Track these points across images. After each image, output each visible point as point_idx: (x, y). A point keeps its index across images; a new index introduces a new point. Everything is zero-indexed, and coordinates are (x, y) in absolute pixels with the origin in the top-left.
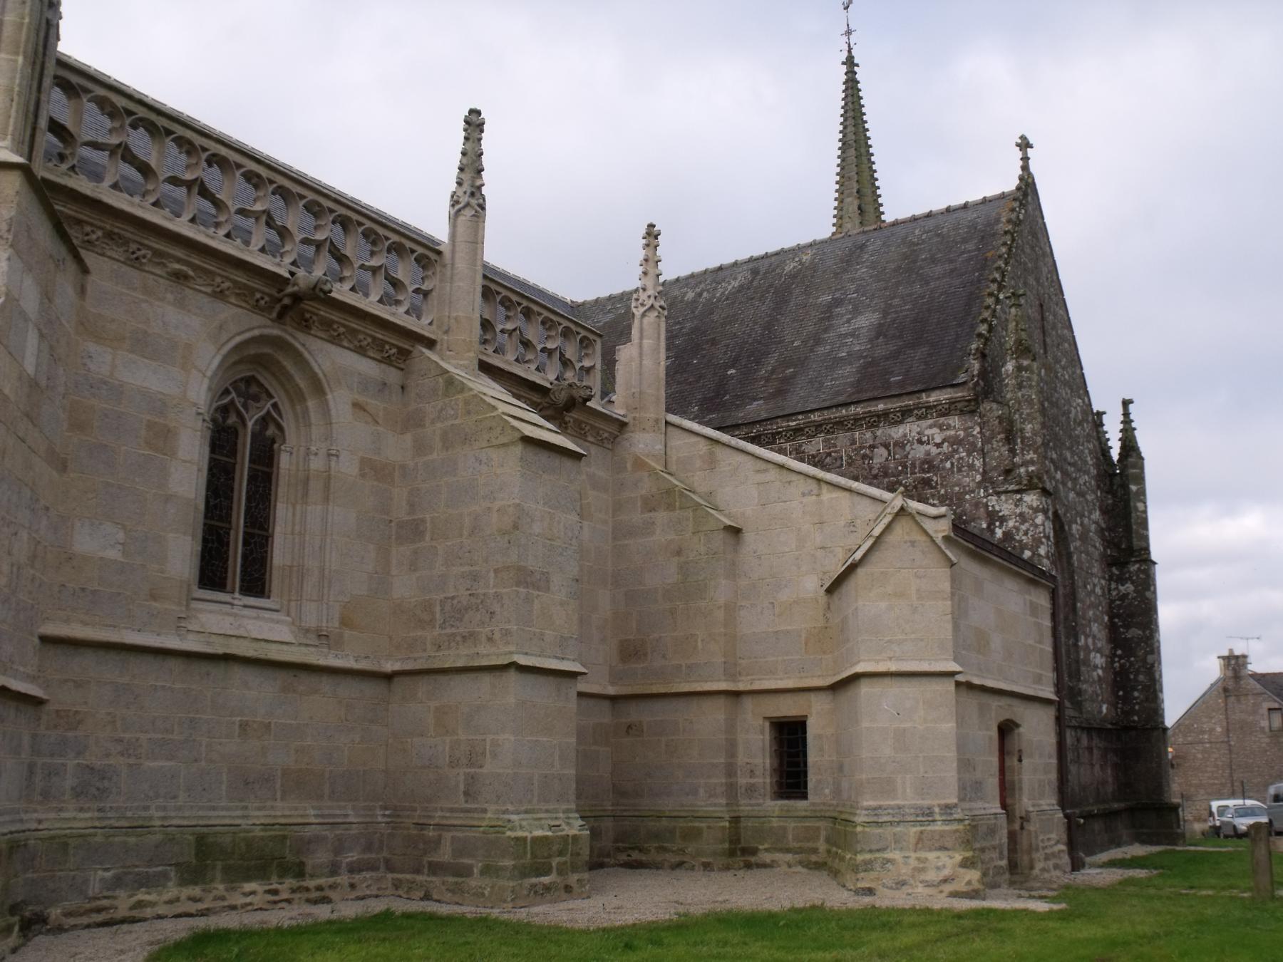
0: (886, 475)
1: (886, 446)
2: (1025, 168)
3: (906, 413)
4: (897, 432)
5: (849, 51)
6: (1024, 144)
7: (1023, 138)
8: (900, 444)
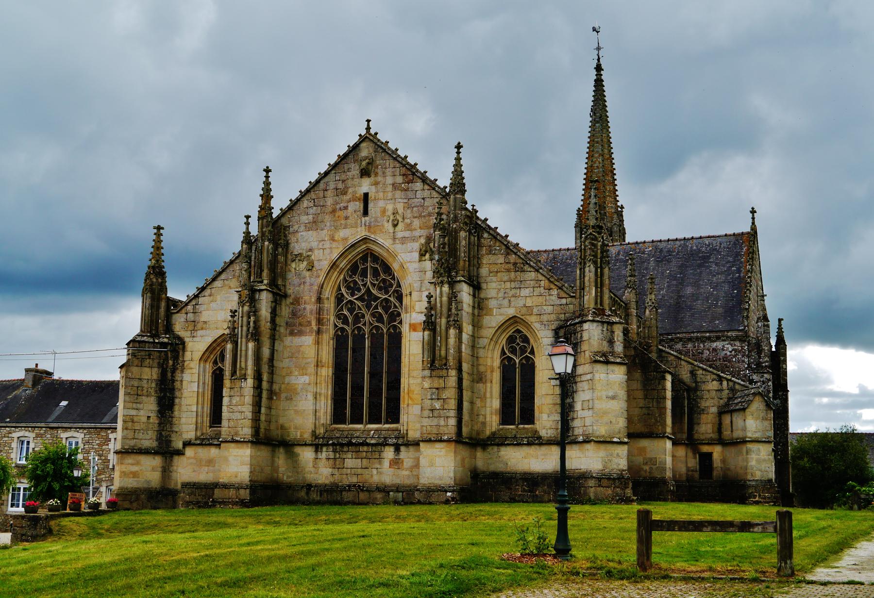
0: (708, 361)
1: (709, 350)
2: (753, 223)
3: (718, 338)
4: (714, 345)
5: (599, 60)
6: (753, 212)
7: (753, 208)
8: (715, 350)
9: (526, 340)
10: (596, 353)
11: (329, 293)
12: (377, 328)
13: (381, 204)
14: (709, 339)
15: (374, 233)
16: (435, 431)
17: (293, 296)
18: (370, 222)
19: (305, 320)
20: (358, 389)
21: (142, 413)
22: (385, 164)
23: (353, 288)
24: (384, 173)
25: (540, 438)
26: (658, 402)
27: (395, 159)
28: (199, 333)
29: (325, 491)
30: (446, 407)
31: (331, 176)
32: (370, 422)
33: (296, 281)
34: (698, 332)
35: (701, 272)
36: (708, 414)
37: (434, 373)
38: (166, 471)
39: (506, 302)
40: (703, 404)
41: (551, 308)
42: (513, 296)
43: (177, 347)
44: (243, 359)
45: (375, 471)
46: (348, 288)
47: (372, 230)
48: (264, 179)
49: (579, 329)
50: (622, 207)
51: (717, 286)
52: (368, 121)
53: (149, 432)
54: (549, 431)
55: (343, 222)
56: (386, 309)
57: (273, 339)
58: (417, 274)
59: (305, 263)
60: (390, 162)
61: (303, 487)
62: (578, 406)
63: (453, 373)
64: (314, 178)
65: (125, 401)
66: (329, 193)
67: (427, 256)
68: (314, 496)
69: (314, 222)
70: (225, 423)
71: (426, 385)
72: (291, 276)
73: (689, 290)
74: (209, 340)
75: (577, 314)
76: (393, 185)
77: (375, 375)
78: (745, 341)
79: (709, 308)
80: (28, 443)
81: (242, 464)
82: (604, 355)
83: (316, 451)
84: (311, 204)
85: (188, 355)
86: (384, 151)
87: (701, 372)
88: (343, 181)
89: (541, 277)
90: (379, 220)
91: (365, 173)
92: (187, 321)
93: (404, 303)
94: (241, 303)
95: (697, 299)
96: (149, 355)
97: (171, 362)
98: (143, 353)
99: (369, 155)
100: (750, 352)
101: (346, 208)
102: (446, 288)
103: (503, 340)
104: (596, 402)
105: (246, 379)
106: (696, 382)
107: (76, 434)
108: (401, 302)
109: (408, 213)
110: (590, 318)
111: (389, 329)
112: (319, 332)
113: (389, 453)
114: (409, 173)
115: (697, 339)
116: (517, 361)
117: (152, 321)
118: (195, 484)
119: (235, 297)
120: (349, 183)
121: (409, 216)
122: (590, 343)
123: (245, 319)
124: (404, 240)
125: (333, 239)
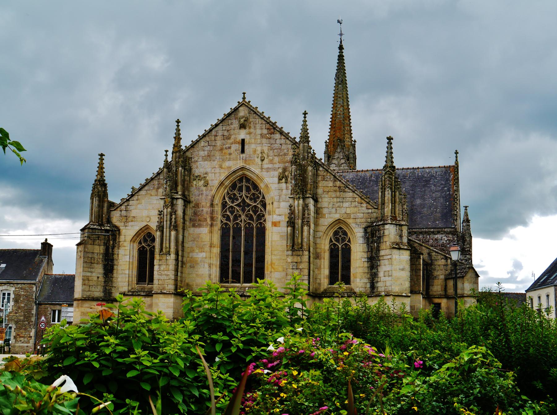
1: (433, 239)
2: (456, 160)
3: (439, 232)
4: (436, 236)
5: (341, 42)
7: (456, 151)
8: (436, 240)
9: (345, 233)
10: (393, 243)
11: (218, 201)
12: (249, 224)
13: (253, 146)
14: (433, 233)
15: (249, 164)
17: (194, 202)
20: (236, 261)
21: (94, 274)
22: (255, 121)
23: (233, 198)
24: (255, 127)
25: (355, 293)
26: (416, 272)
27: (262, 118)
28: (130, 224)
31: (220, 127)
33: (197, 193)
34: (426, 228)
35: (425, 190)
36: (438, 279)
37: (294, 253)
39: (334, 210)
40: (436, 273)
41: (362, 215)
42: (339, 207)
43: (115, 232)
44: (168, 242)
46: (230, 198)
48: (176, 127)
49: (382, 228)
50: (355, 141)
51: (436, 199)
52: (244, 93)
53: (98, 287)
55: (228, 156)
56: (255, 212)
57: (184, 229)
58: (277, 191)
59: (203, 182)
60: (259, 120)
62: (381, 274)
63: (306, 253)
64: (208, 128)
66: (218, 138)
69: (208, 156)
70: (155, 282)
71: (289, 260)
72: (193, 189)
73: (418, 202)
74: (137, 228)
75: (380, 219)
76: (261, 135)
77: (248, 253)
78: (455, 235)
79: (432, 213)
80: (9, 294)
81: (168, 307)
82: (397, 244)
84: (207, 144)
85: (122, 238)
86: (255, 113)
87: (434, 253)
88: (228, 131)
89: (356, 196)
90: (252, 156)
91: (243, 126)
92: (121, 216)
93: (267, 209)
94: (166, 206)
95: (424, 208)
96: (98, 237)
97: (111, 242)
98: (95, 236)
99: (243, 115)
100: (458, 241)
101: (230, 148)
102: (301, 201)
103: (331, 234)
104: (394, 272)
105: (170, 254)
106: (431, 260)
107: (9, 288)
108: (265, 209)
109: (271, 153)
110: (390, 222)
111: (257, 225)
112: (212, 225)
114: (271, 128)
115: (426, 232)
116: (340, 246)
117: (99, 216)
119: (162, 202)
120: (232, 132)
121: (272, 154)
122: (389, 237)
123: (168, 216)
124: (268, 170)
125: (221, 167)
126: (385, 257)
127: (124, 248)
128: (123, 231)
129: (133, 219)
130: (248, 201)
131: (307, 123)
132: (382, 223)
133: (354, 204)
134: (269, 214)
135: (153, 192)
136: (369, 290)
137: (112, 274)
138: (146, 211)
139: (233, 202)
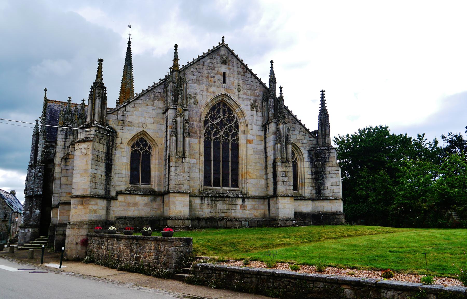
11: (203, 118)
15: (229, 92)
16: (285, 192)
18: (227, 87)
19: (193, 130)
21: (99, 172)
25: (304, 197)
28: (127, 128)
29: (208, 221)
30: (289, 180)
31: (206, 59)
32: (223, 186)
37: (283, 164)
38: (108, 209)
45: (233, 211)
46: (211, 117)
47: (228, 91)
52: (223, 37)
53: (102, 185)
54: (308, 194)
55: (213, 83)
59: (193, 100)
60: (235, 60)
61: (195, 219)
65: (92, 164)
66: (205, 67)
67: (255, 109)
68: (203, 224)
81: (185, 205)
83: (202, 200)
84: (195, 70)
85: (119, 140)
88: (212, 63)
91: (224, 62)
96: (103, 137)
98: (100, 135)
101: (214, 77)
105: (185, 158)
113: (240, 202)
118: (125, 218)
123: (182, 124)
125: (207, 91)
126: (331, 172)
127: (121, 150)
128: (120, 134)
129: (130, 124)
130: (225, 120)
131: (274, 69)
132: (326, 148)
133: (301, 133)
134: (244, 133)
135: (149, 103)
136: (314, 196)
137: (111, 173)
138: (143, 119)
139: (213, 121)
